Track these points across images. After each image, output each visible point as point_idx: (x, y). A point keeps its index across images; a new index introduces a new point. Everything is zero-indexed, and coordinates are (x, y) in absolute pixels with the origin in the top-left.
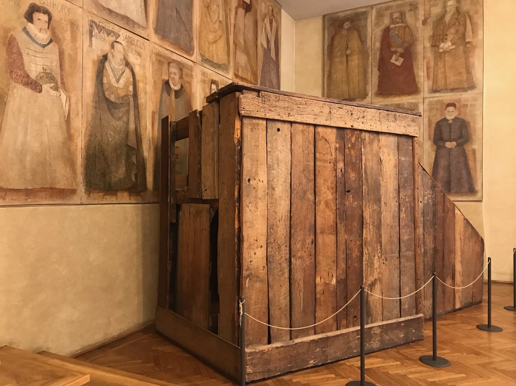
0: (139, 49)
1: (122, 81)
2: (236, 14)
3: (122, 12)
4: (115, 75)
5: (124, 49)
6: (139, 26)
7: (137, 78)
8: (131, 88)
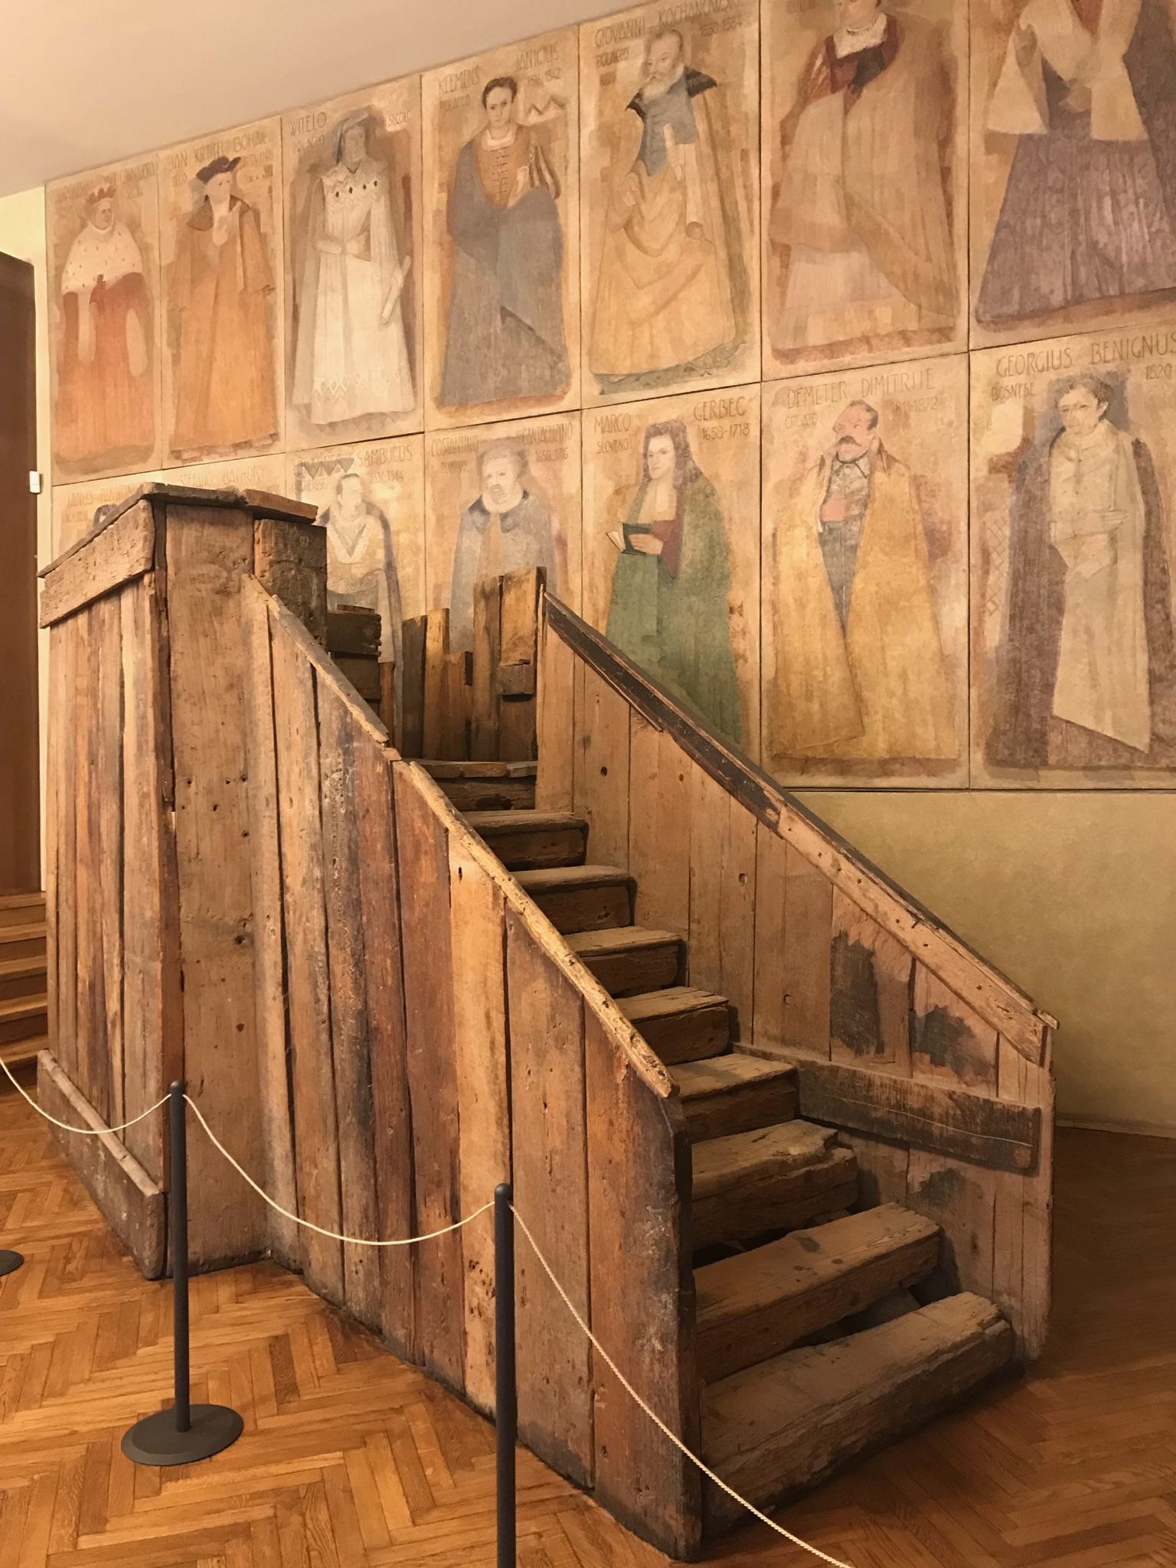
0: (396, 466)
1: (360, 549)
2: (786, 140)
3: (358, 412)
4: (345, 542)
5: (362, 484)
6: (395, 415)
7: (393, 527)
8: (381, 554)
